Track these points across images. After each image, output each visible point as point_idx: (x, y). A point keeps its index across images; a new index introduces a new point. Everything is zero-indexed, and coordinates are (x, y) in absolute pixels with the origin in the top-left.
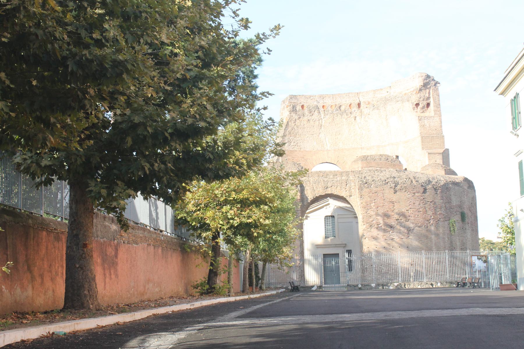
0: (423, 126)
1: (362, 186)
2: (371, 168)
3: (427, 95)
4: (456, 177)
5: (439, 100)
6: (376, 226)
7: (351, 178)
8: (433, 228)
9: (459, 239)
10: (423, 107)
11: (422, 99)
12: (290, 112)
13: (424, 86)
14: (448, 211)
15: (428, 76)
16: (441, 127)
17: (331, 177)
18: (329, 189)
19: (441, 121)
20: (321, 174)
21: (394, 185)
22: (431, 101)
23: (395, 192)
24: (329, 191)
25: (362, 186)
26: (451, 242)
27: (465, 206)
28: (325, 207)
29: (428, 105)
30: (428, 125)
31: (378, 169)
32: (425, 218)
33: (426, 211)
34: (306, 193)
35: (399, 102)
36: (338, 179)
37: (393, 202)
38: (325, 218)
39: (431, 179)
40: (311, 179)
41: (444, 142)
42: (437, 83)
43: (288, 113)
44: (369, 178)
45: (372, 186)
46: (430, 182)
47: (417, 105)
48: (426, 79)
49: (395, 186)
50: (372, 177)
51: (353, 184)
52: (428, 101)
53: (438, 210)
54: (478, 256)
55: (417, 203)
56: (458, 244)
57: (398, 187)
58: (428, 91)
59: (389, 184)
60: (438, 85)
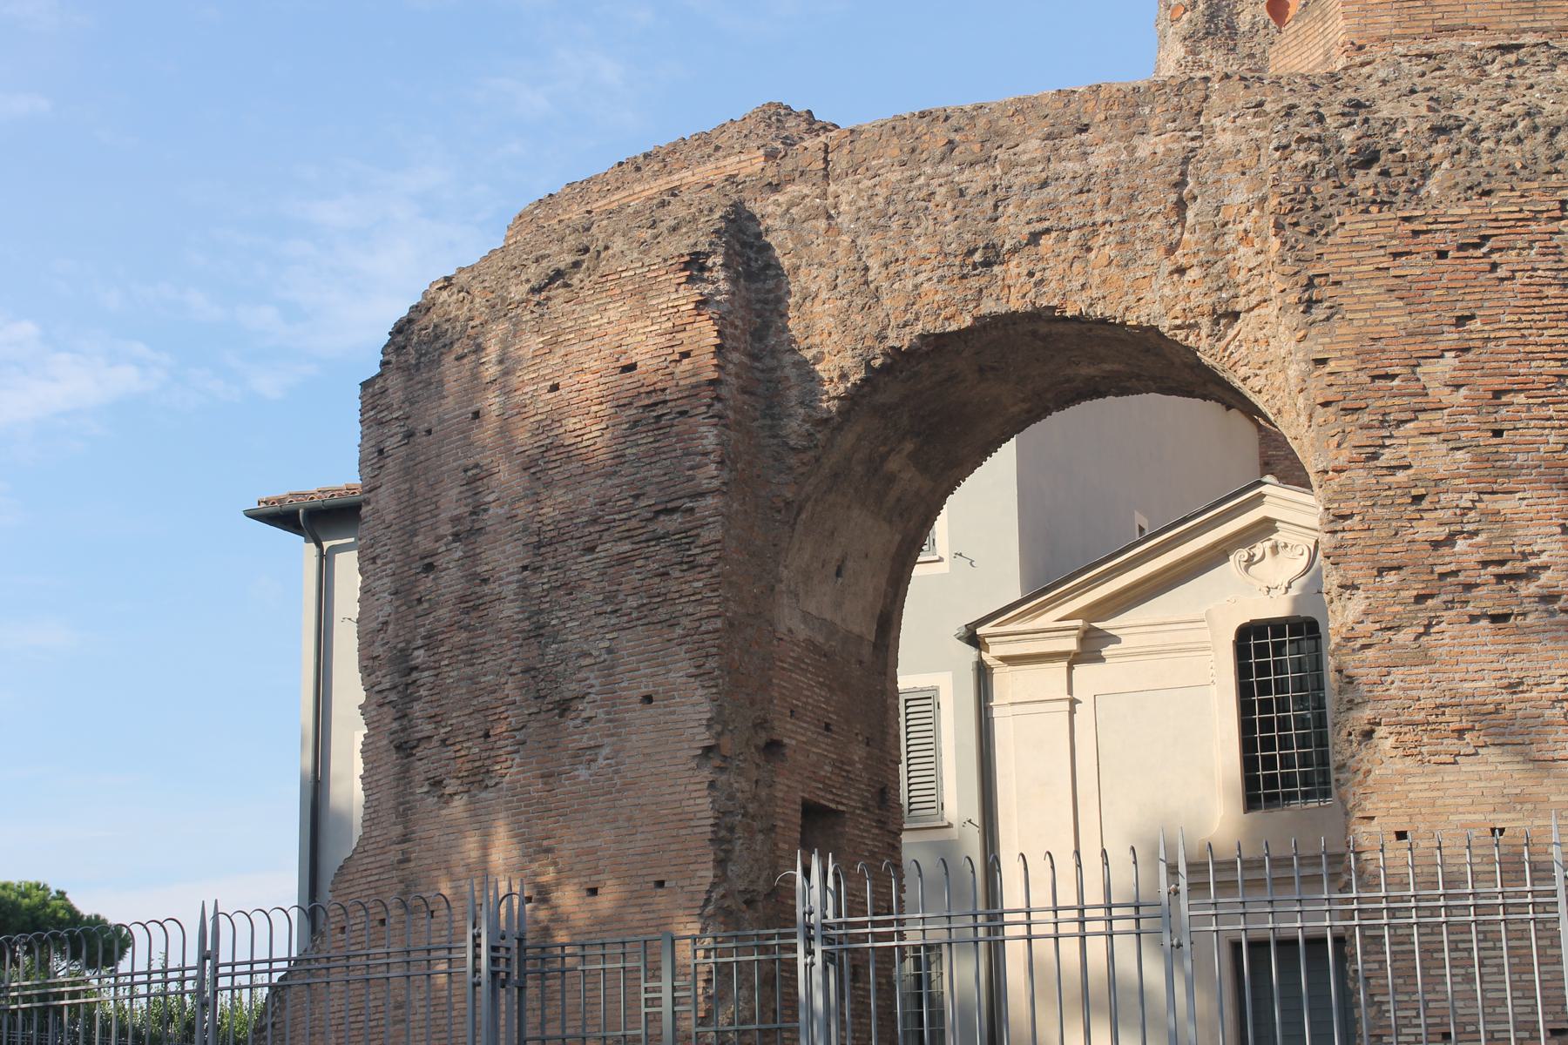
1: (1322, 189)
6: (1487, 598)
7: (1225, 140)
12: (1192, 40)
17: (1033, 147)
18: (1015, 268)
20: (941, 133)
24: (1011, 292)
25: (1322, 189)
28: (1242, 554)
31: (1528, 39)
34: (794, 325)
36: (1100, 159)
40: (845, 194)
43: (1179, 51)
44: (1408, 116)
45: (1432, 187)
50: (1435, 103)
51: (1240, 195)
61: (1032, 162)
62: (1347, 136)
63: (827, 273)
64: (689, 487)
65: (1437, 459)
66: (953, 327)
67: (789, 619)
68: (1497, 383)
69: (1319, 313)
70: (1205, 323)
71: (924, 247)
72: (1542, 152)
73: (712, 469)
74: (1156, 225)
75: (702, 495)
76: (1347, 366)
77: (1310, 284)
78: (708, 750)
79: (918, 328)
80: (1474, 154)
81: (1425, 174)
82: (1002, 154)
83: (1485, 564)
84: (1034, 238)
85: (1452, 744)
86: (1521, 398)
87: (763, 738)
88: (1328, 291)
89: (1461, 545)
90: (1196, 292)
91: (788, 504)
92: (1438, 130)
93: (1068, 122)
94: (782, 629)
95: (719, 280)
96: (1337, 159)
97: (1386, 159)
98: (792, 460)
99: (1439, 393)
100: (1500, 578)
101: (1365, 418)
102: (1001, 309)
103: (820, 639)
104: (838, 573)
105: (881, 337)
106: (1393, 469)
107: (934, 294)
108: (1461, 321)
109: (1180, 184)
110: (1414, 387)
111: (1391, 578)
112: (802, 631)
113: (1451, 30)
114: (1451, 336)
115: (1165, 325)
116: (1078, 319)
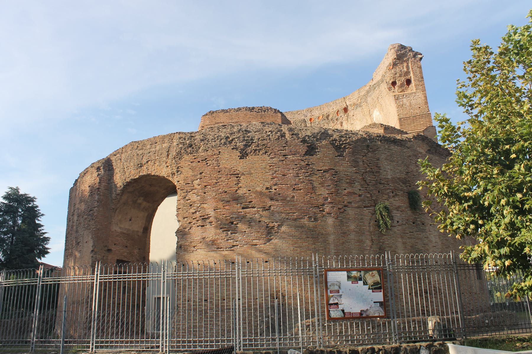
0: (400, 107)
3: (405, 69)
5: (421, 72)
6: (200, 223)
8: (330, 221)
9: (404, 243)
10: (402, 86)
11: (398, 75)
13: (398, 59)
14: (371, 188)
15: (402, 47)
16: (426, 103)
17: (149, 147)
18: (144, 168)
19: (426, 97)
21: (244, 143)
22: (412, 75)
23: (244, 155)
25: (182, 151)
29: (409, 82)
30: (408, 104)
32: (308, 202)
33: (313, 188)
35: (376, 89)
36: (158, 148)
37: (237, 176)
39: (330, 132)
42: (416, 54)
45: (200, 150)
46: (325, 134)
47: (394, 84)
48: (401, 51)
49: (246, 146)
52: (408, 77)
53: (345, 185)
54: (348, 271)
55: (291, 174)
57: (253, 147)
58: (405, 64)
59: (233, 142)
60: (420, 56)
62: (188, 142)
63: (119, 169)
64: (93, 206)
67: (115, 228)
68: (205, 184)
69: (179, 173)
70: (171, 175)
71: (132, 164)
72: (218, 143)
73: (96, 203)
74: (164, 159)
75: (95, 207)
77: (178, 168)
78: (92, 251)
80: (207, 144)
81: (199, 148)
82: (144, 148)
83: (201, 216)
84: (147, 162)
86: (209, 187)
87: (106, 248)
88: (181, 169)
89: (197, 213)
90: (169, 170)
91: (113, 209)
92: (202, 140)
93: (154, 142)
94: (113, 230)
95: (102, 171)
96: (186, 146)
97: (194, 145)
98: (114, 201)
99: (196, 186)
100: (203, 219)
101: (184, 191)
102: (143, 174)
103: (125, 232)
104: (130, 220)
105: (125, 180)
106: (187, 200)
107: (133, 172)
108: (201, 173)
109: (168, 152)
110: (192, 185)
111: (186, 219)
112: (119, 230)
113: (218, 123)
114: (199, 176)
115: (165, 176)
116: (154, 175)
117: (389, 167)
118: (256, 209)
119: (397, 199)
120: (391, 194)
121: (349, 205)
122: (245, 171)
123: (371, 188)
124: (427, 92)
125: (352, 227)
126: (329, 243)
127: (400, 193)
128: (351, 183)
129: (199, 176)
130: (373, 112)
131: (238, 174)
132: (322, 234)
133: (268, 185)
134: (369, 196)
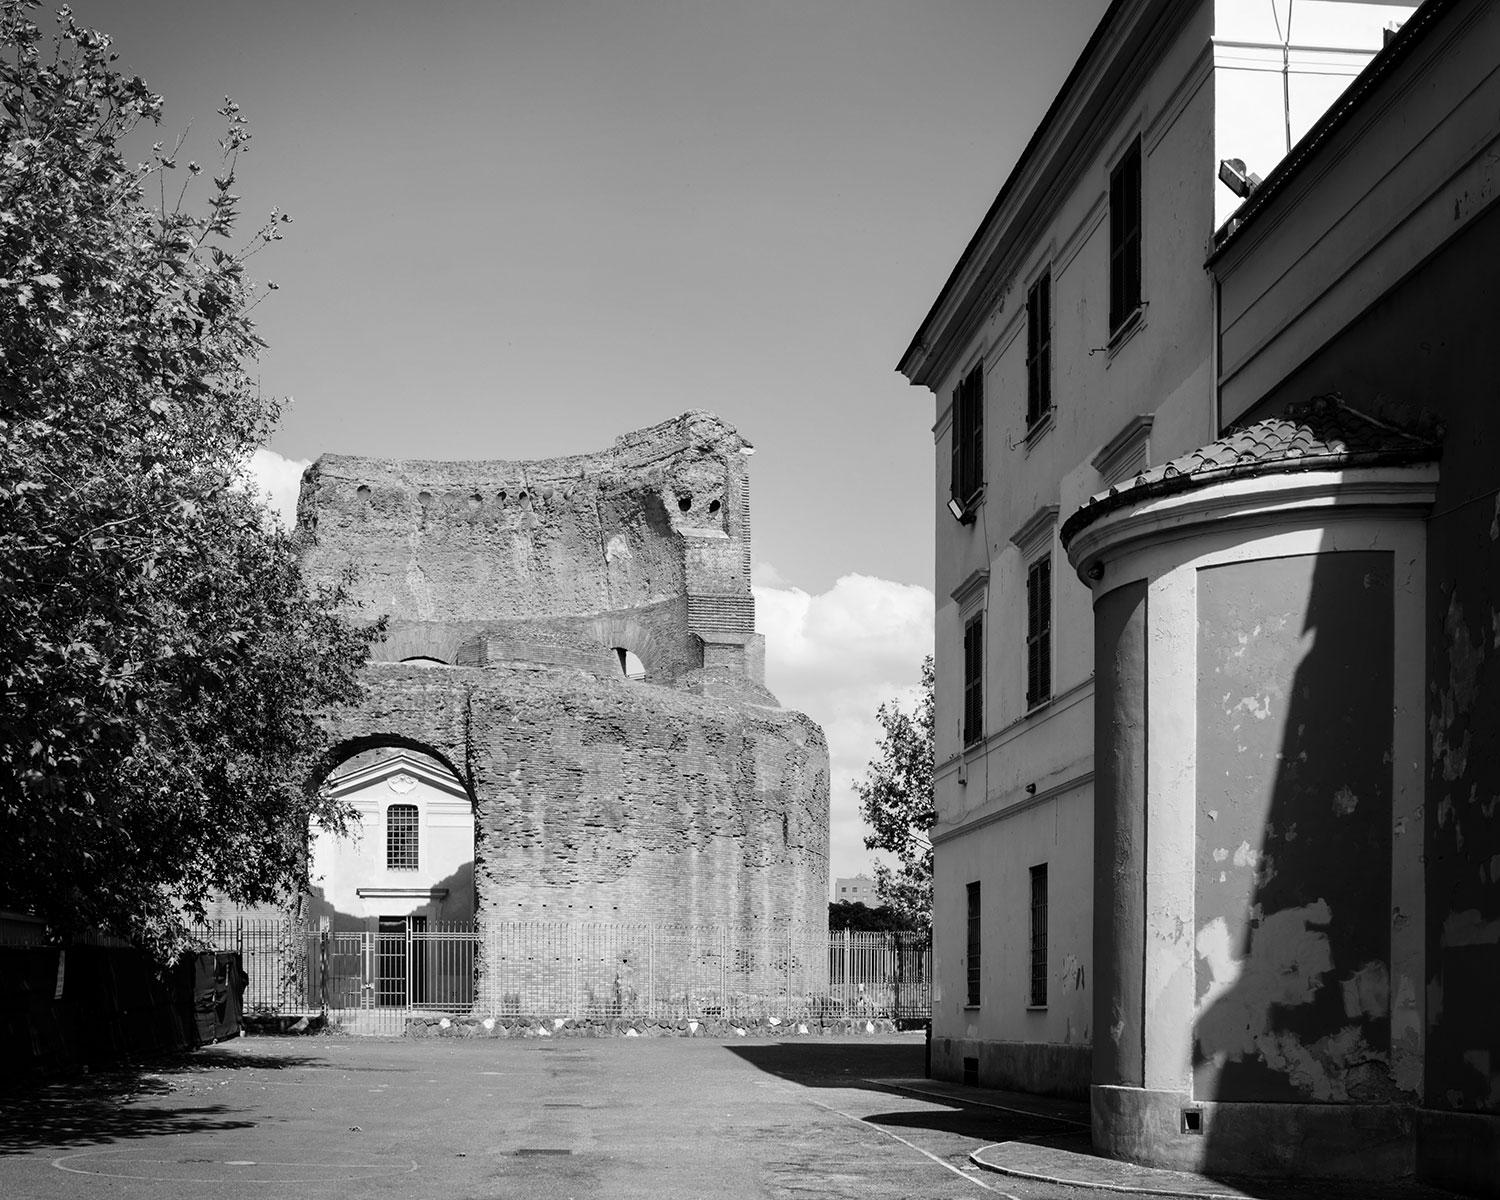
2: (518, 665)
4: (778, 710)
14: (744, 807)
16: (747, 571)
18: (384, 720)
24: (386, 727)
26: (747, 900)
27: (794, 798)
30: (710, 565)
31: (542, 667)
37: (578, 771)
38: (389, 814)
41: (751, 616)
56: (767, 904)
61: (393, 687)
65: (513, 801)
66: (364, 735)
76: (490, 770)
79: (355, 734)
85: (509, 881)
117: (764, 774)
118: (602, 829)
119: (768, 824)
120: (764, 817)
121: (717, 831)
122: (590, 768)
123: (744, 807)
124: (753, 544)
125: (718, 865)
126: (691, 888)
127: (773, 815)
128: (720, 800)
129: (518, 765)
130: (608, 540)
131: (580, 770)
132: (684, 873)
133: (621, 792)
134: (740, 819)
